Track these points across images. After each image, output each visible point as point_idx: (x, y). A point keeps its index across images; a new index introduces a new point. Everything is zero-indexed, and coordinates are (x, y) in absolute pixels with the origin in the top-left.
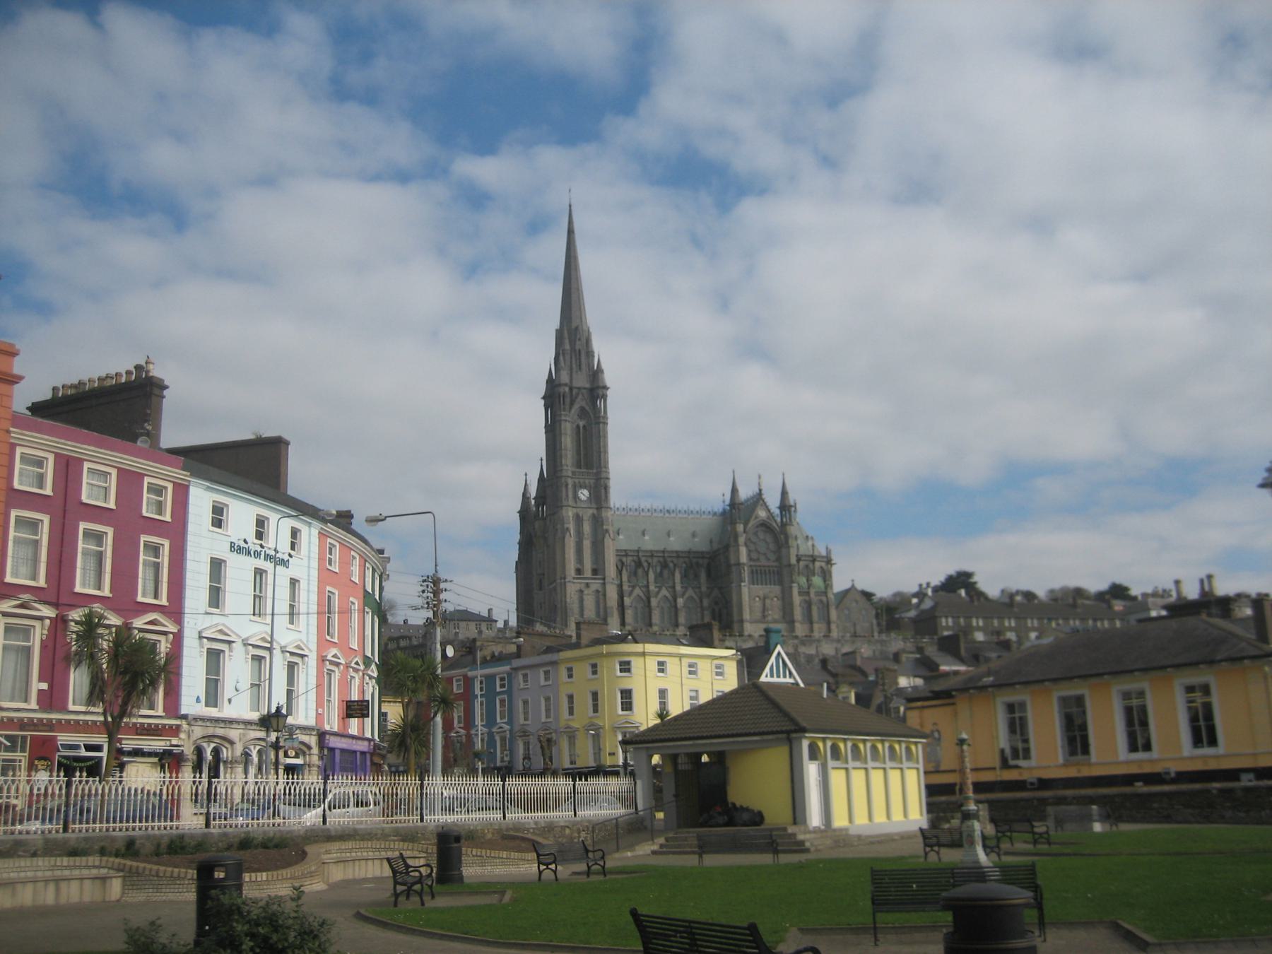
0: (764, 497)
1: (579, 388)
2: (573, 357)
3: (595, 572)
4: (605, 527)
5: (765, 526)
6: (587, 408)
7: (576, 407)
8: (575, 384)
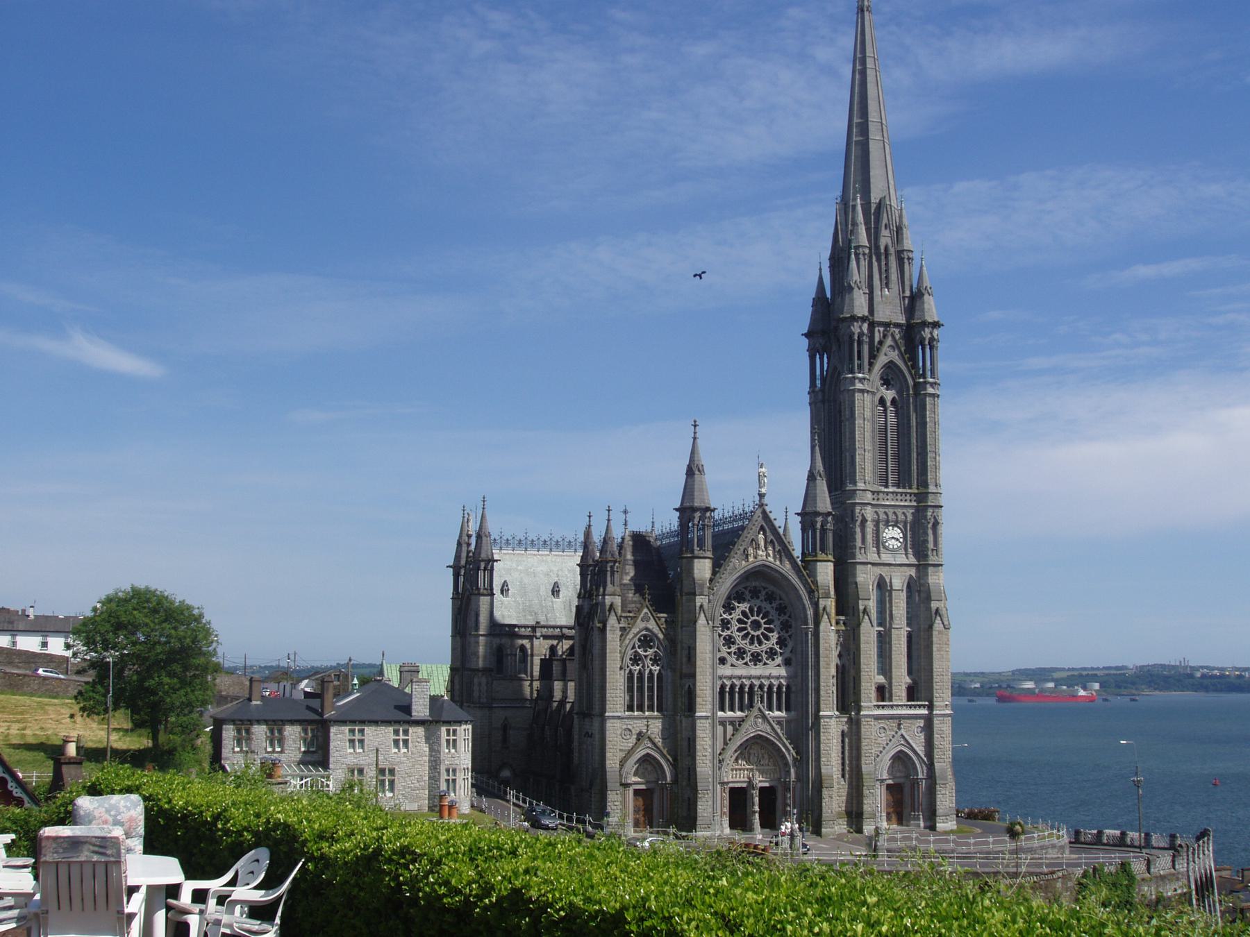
1: (887, 325)
2: (875, 264)
3: (912, 693)
4: (934, 605)
7: (882, 360)
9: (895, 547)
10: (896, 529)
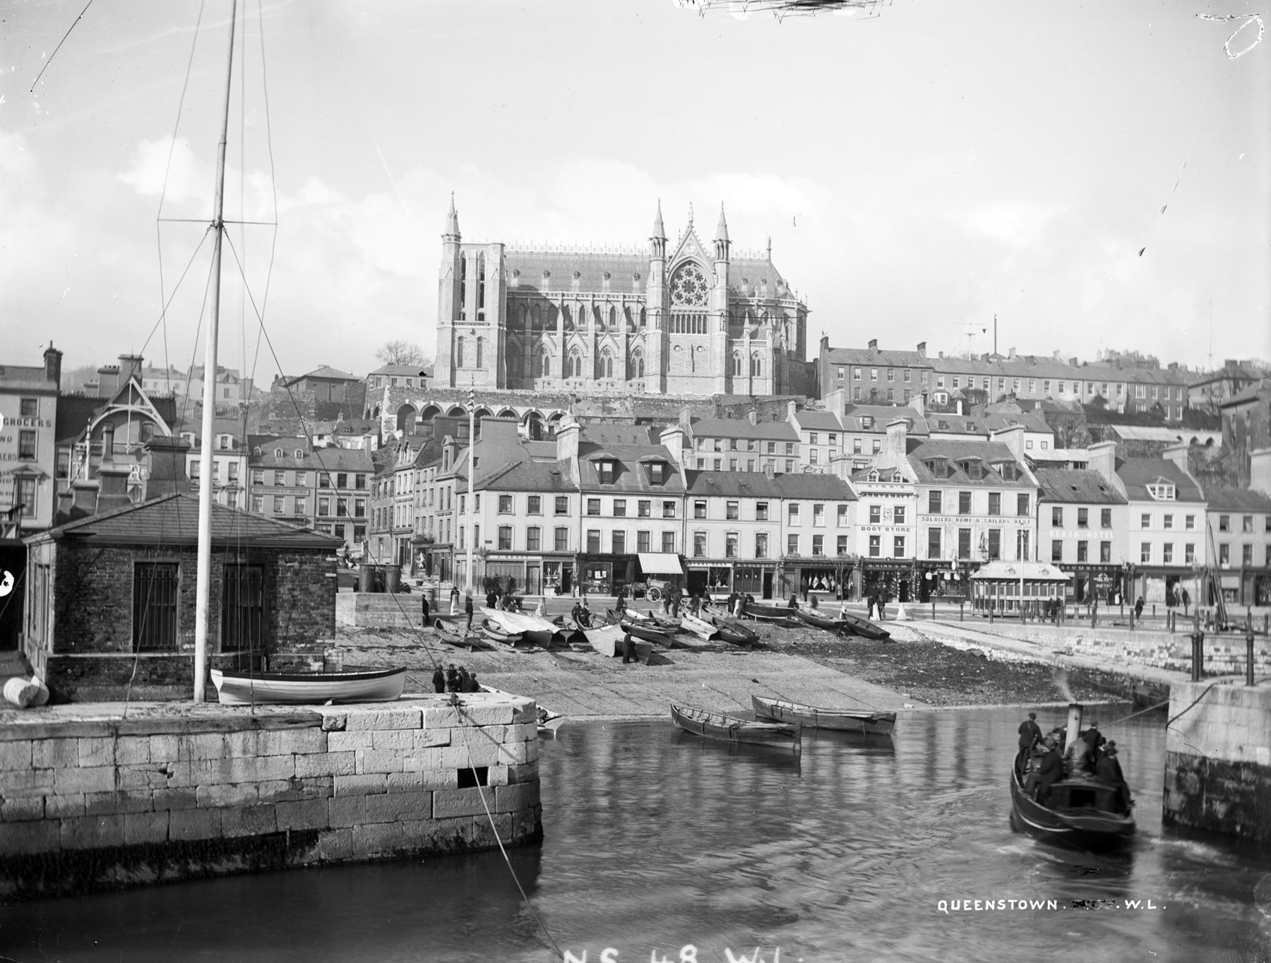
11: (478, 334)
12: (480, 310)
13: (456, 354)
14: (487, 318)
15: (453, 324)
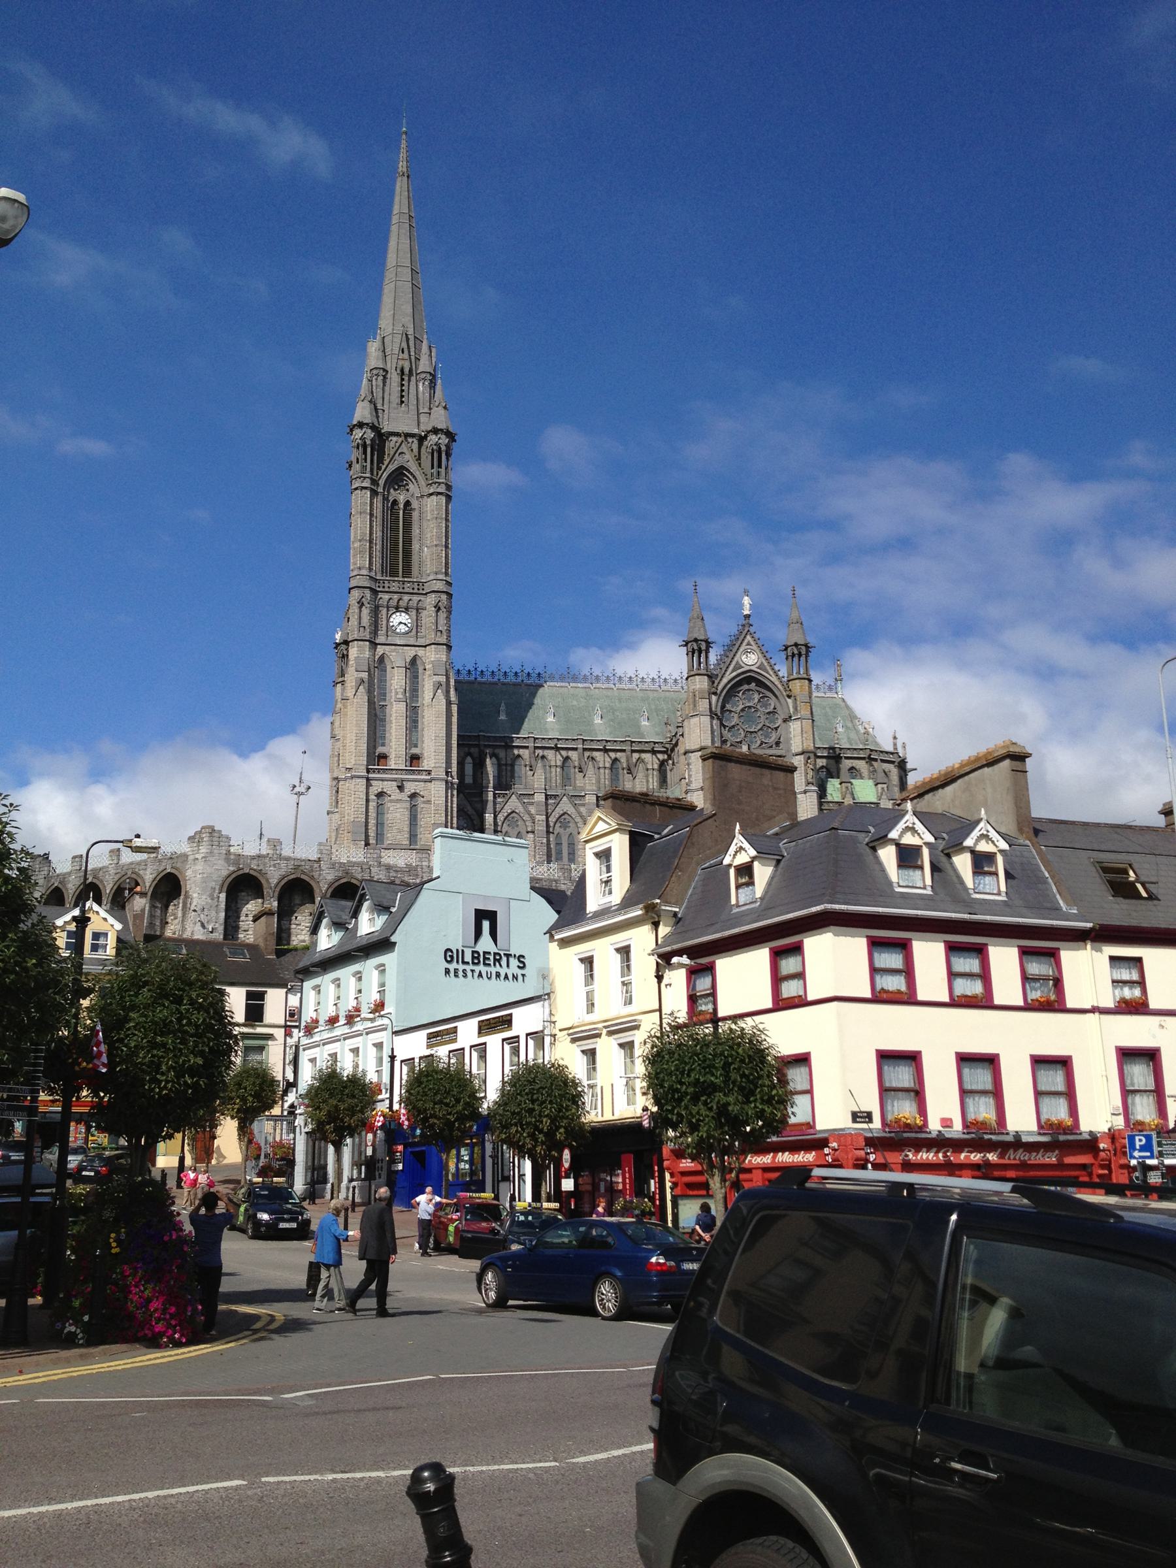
0: (752, 629)
5: (749, 679)
6: (413, 466)
8: (386, 427)
9: (403, 631)
10: (403, 614)
11: (410, 787)
12: (414, 751)
13: (372, 822)
14: (426, 764)
15: (368, 771)
